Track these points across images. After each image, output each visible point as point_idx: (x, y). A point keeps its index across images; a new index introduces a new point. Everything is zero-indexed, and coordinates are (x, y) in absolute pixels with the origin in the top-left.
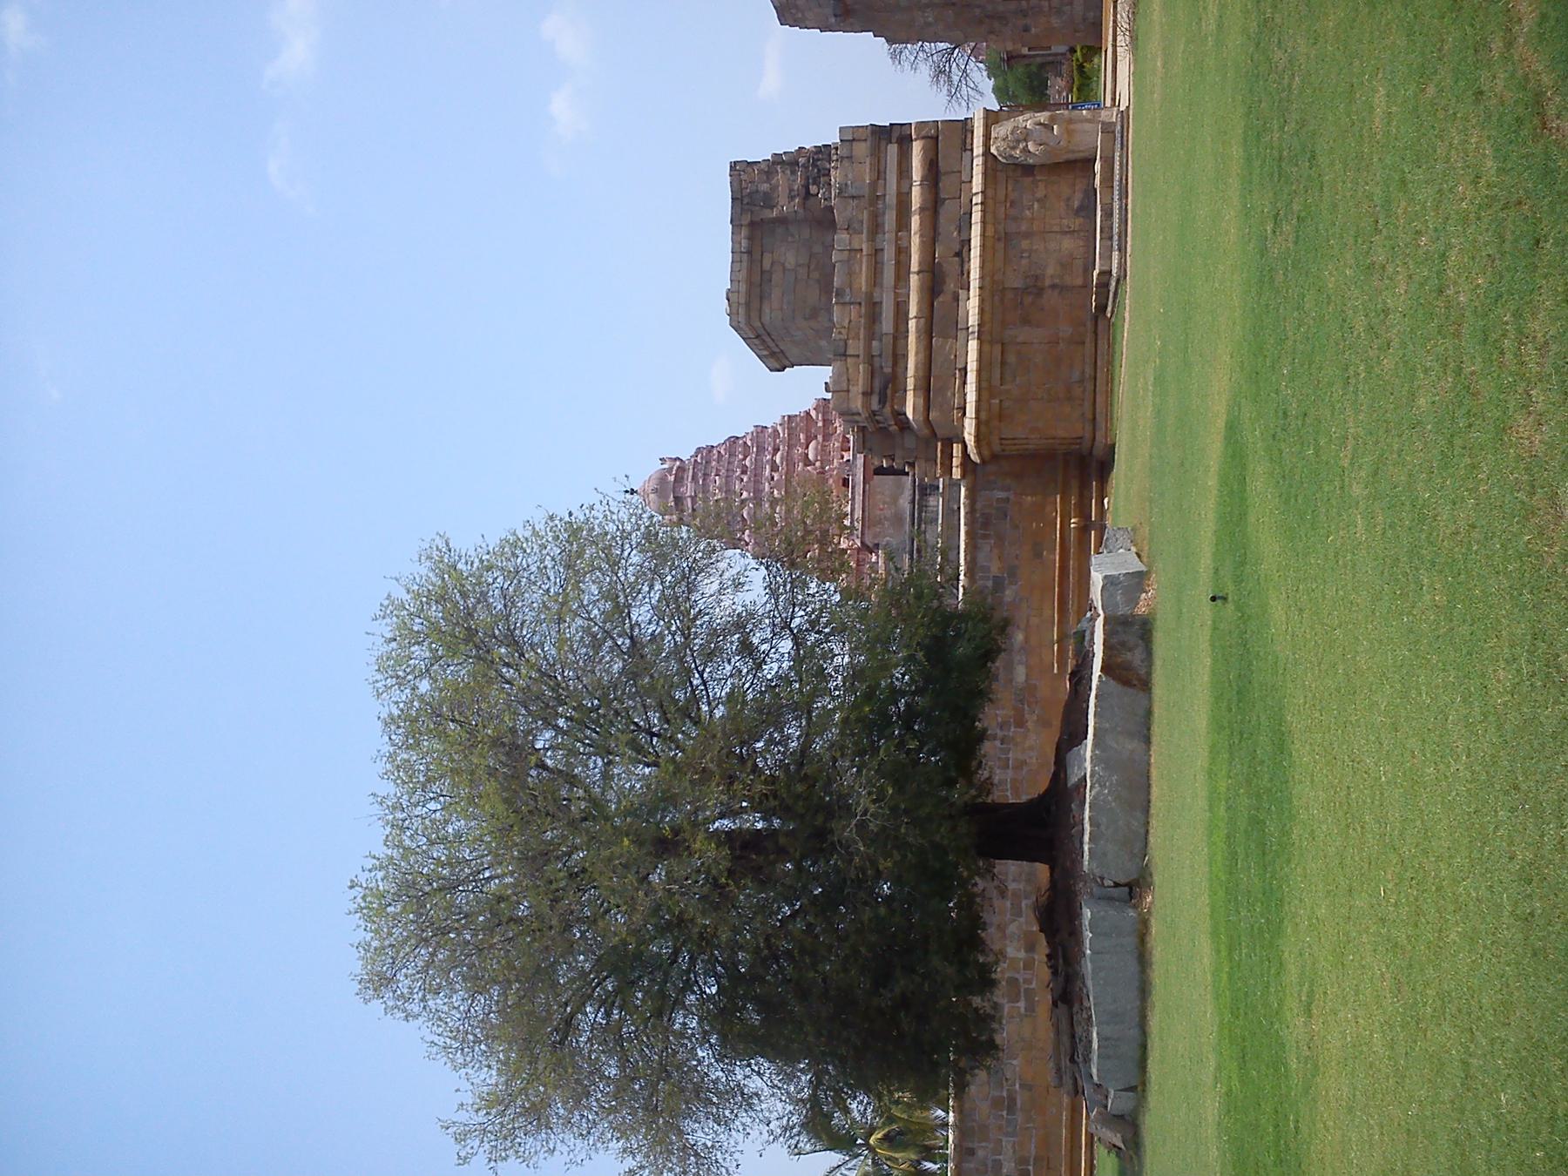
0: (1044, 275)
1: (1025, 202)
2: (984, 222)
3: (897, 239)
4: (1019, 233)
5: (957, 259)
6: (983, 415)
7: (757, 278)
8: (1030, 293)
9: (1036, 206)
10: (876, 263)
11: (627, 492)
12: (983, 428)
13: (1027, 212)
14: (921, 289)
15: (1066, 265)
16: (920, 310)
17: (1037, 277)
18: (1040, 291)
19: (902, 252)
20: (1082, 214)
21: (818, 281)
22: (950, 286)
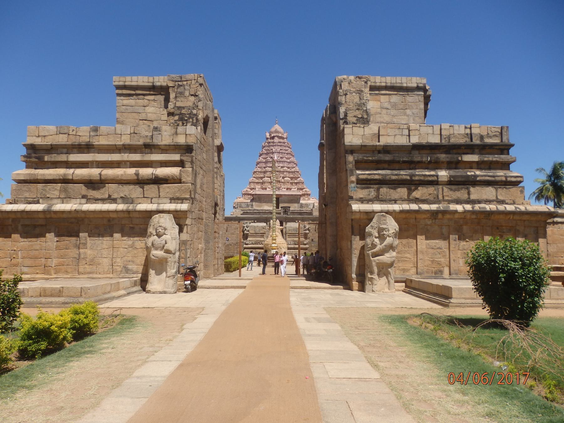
0: (86, 248)
5: (107, 196)
16: (78, 176)
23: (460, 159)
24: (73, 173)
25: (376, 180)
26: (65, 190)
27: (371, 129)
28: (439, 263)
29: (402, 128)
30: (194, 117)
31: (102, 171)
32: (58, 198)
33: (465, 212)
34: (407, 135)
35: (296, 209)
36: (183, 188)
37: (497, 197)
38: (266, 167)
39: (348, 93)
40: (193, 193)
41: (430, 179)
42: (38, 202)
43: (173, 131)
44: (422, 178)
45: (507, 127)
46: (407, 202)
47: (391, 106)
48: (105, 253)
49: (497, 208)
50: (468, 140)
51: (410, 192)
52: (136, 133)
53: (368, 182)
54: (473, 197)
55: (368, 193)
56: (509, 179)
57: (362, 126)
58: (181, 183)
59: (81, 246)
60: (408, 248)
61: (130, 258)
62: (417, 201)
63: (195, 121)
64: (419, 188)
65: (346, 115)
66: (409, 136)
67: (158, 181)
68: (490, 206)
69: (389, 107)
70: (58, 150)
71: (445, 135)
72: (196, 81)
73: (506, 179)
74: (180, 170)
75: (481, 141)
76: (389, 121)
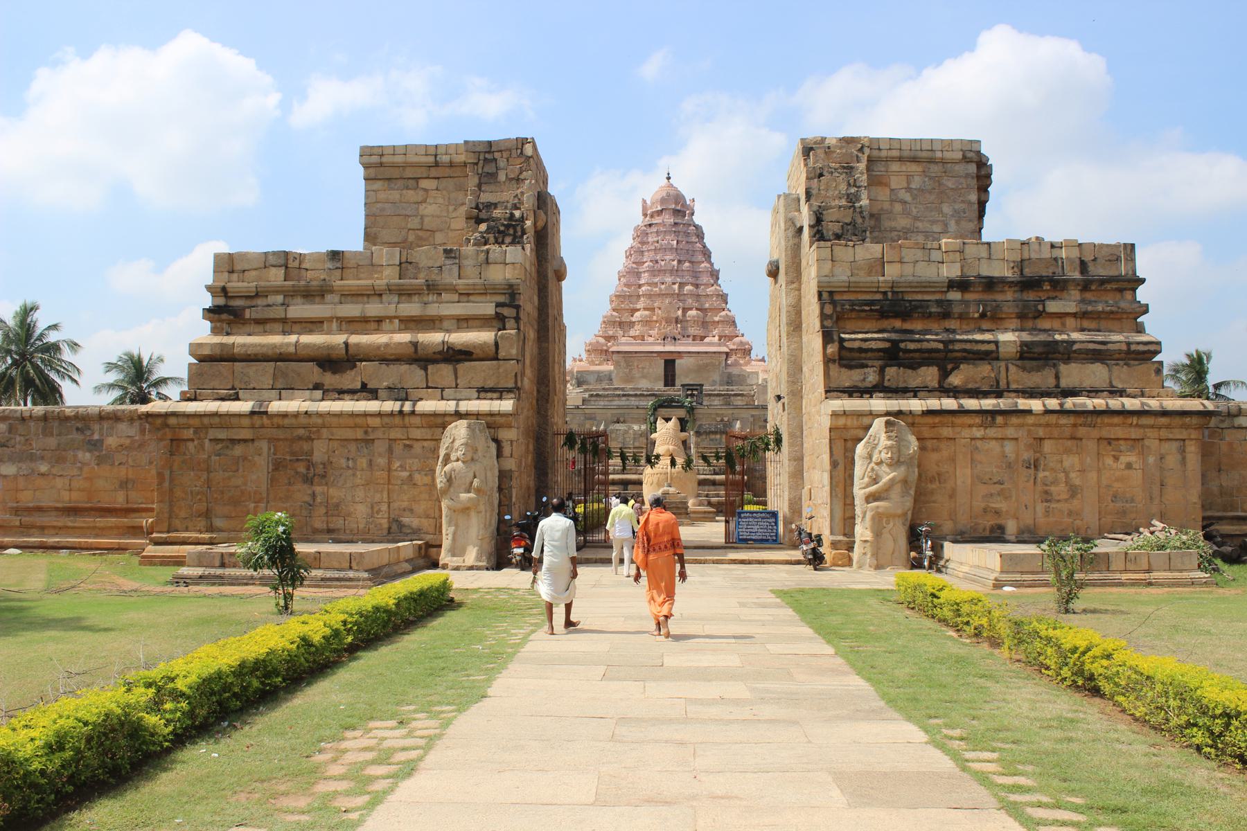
1: (409, 461)
2: (380, 414)
3: (391, 318)
4: (373, 456)
5: (359, 387)
6: (172, 421)
7: (409, 173)
8: (308, 469)
9: (405, 474)
10: (368, 296)
12: (159, 421)
14: (331, 347)
15: (334, 509)
16: (307, 346)
17: (324, 476)
18: (308, 480)
19: (378, 323)
20: (394, 527)
22: (329, 379)
23: (1040, 308)
24: (297, 342)
27: (867, 249)
28: (997, 513)
29: (929, 247)
30: (518, 225)
32: (272, 389)
33: (1048, 412)
34: (939, 262)
36: (501, 370)
38: (643, 285)
39: (825, 173)
40: (519, 378)
42: (237, 398)
43: (482, 256)
44: (968, 346)
46: (937, 394)
47: (911, 195)
48: (360, 494)
49: (1107, 405)
51: (945, 374)
52: (411, 263)
53: (863, 355)
54: (1065, 383)
55: (862, 378)
56: (1133, 347)
57: (851, 244)
58: (497, 359)
59: (316, 480)
60: (937, 482)
61: (405, 504)
62: (955, 393)
63: (520, 233)
64: (962, 366)
68: (1096, 401)
69: (908, 197)
70: (267, 296)
71: (1014, 262)
72: (519, 151)
73: (1129, 349)
74: (496, 335)
76: (908, 226)
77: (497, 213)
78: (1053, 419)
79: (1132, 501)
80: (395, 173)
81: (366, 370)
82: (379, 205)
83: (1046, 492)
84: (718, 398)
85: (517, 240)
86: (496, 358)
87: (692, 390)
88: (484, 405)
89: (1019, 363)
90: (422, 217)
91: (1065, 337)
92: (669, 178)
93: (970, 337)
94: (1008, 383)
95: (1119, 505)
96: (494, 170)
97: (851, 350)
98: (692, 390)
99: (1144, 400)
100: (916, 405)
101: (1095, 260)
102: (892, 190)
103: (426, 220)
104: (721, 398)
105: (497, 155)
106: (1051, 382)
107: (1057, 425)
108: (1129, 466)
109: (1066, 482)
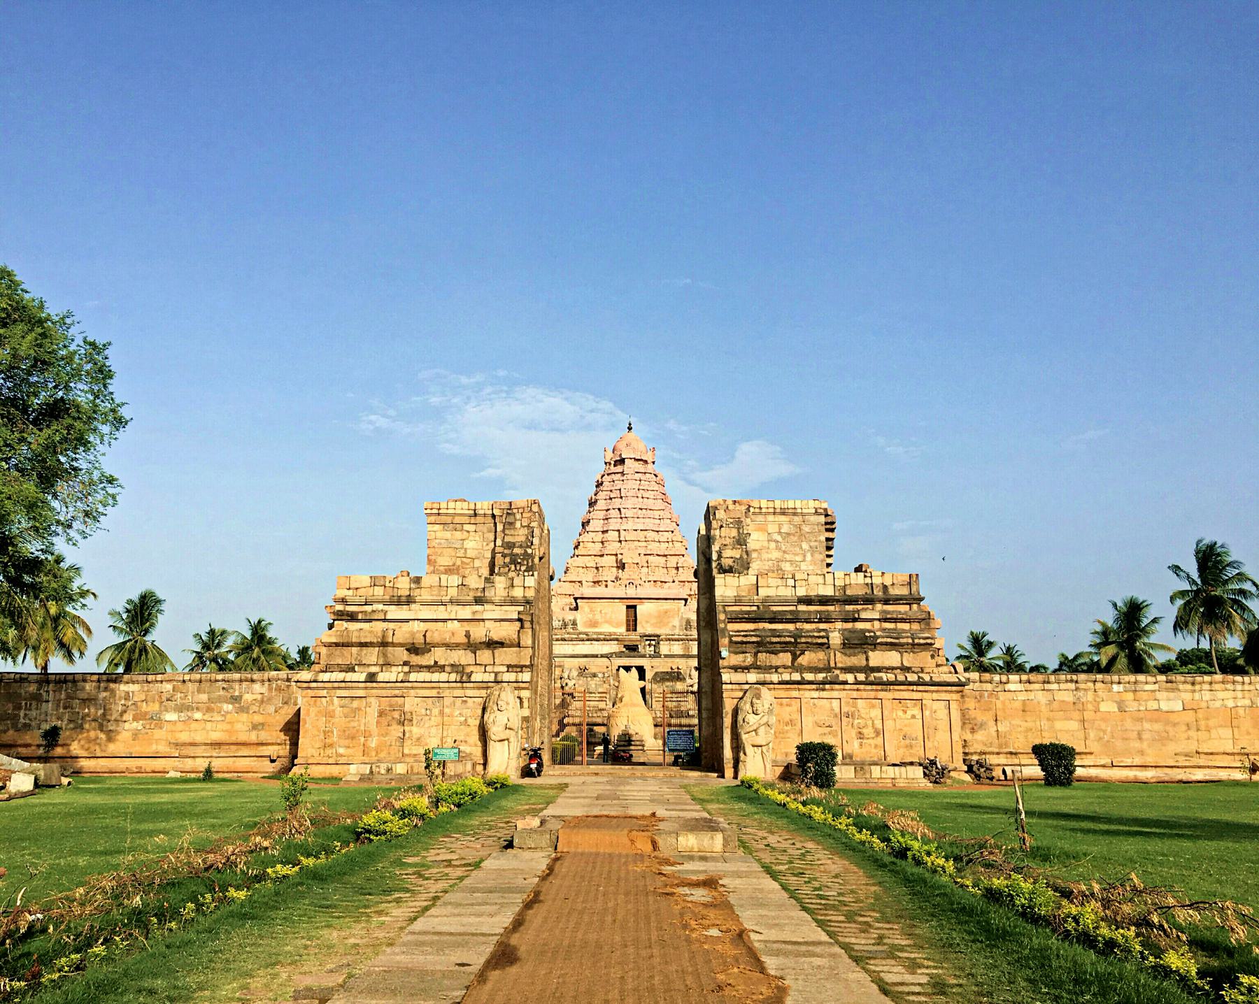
1: (465, 711)
5: (433, 663)
7: (457, 520)
9: (463, 719)
11: (630, 424)
13: (458, 712)
17: (411, 721)
21: (454, 565)
22: (416, 660)
23: (856, 616)
25: (753, 643)
26: (385, 655)
31: (426, 631)
35: (677, 631)
37: (902, 663)
38: (607, 531)
41: (820, 641)
43: (509, 583)
44: (810, 640)
45: (917, 575)
46: (790, 670)
48: (433, 730)
50: (869, 591)
51: (795, 658)
54: (872, 664)
56: (916, 641)
57: (737, 575)
58: (520, 647)
62: (801, 669)
65: (720, 557)
66: (795, 587)
67: (492, 645)
68: (888, 675)
69: (779, 538)
75: (884, 593)
77: (517, 551)
78: (862, 687)
79: (916, 739)
80: (449, 520)
81: (439, 655)
82: (437, 541)
83: (860, 733)
84: (677, 643)
85: (530, 569)
86: (519, 645)
87: (651, 640)
88: (511, 676)
89: (842, 651)
90: (466, 549)
91: (872, 634)
92: (630, 429)
93: (811, 634)
94: (835, 663)
95: (908, 742)
96: (513, 521)
97: (736, 643)
98: (651, 640)
99: (920, 675)
100: (775, 678)
101: (893, 584)
102: (769, 534)
103: (468, 551)
104: (681, 642)
105: (515, 511)
106: (864, 663)
107: (865, 690)
108: (913, 717)
109: (873, 726)
